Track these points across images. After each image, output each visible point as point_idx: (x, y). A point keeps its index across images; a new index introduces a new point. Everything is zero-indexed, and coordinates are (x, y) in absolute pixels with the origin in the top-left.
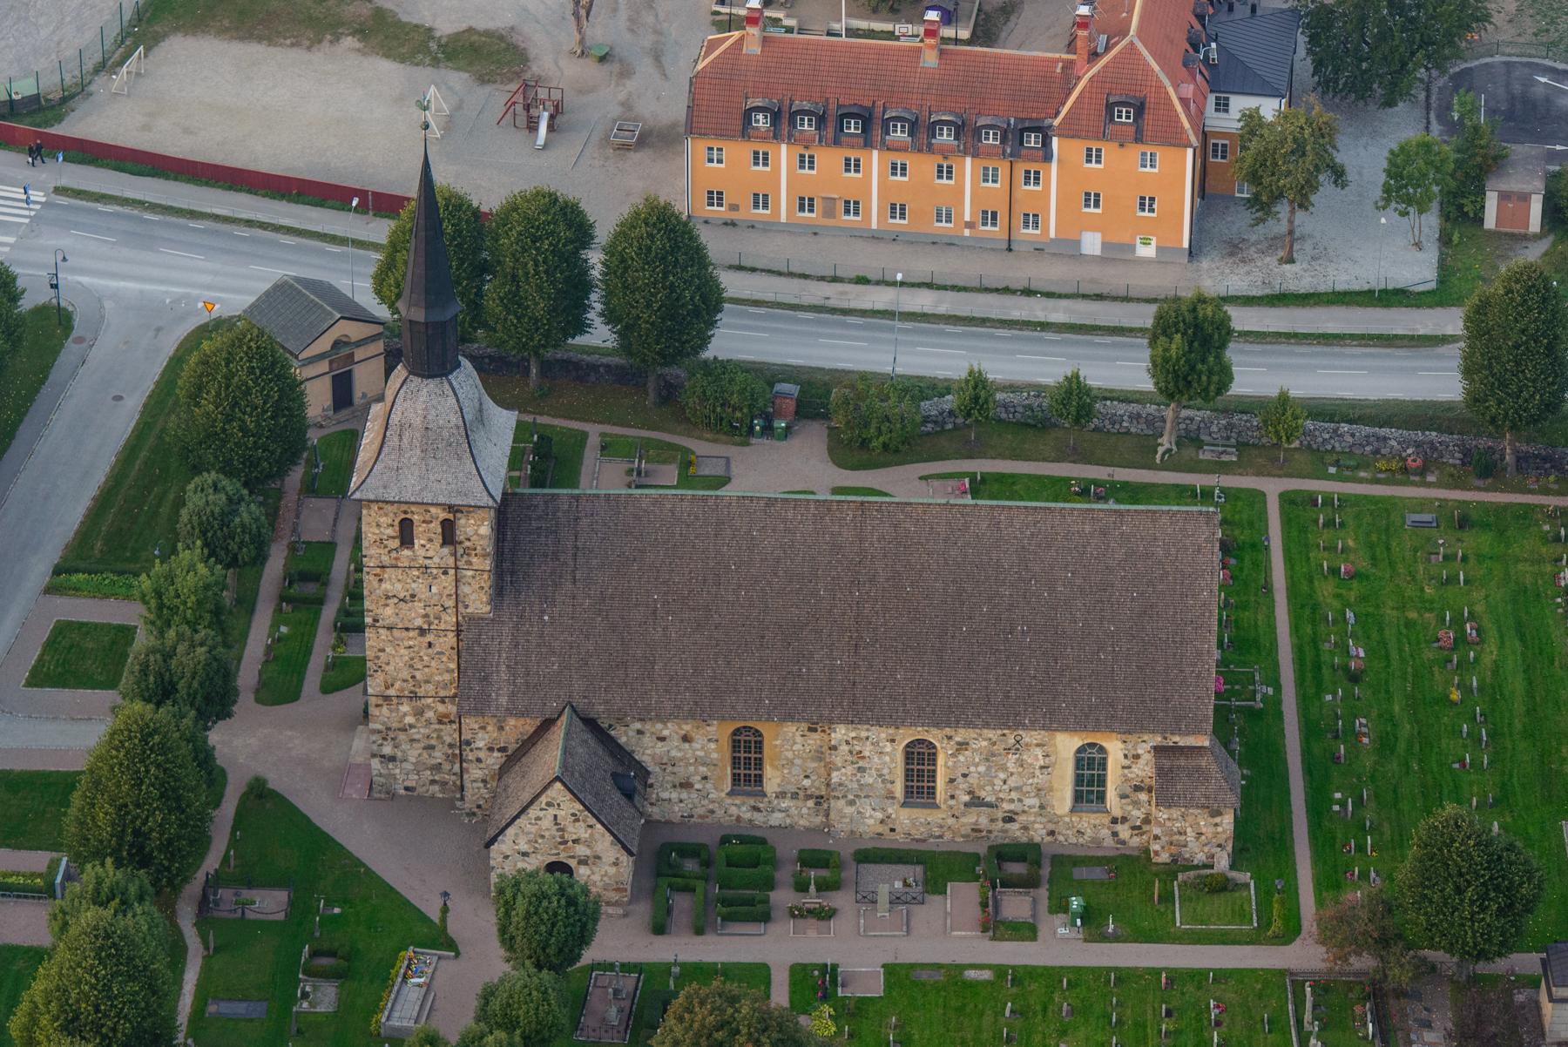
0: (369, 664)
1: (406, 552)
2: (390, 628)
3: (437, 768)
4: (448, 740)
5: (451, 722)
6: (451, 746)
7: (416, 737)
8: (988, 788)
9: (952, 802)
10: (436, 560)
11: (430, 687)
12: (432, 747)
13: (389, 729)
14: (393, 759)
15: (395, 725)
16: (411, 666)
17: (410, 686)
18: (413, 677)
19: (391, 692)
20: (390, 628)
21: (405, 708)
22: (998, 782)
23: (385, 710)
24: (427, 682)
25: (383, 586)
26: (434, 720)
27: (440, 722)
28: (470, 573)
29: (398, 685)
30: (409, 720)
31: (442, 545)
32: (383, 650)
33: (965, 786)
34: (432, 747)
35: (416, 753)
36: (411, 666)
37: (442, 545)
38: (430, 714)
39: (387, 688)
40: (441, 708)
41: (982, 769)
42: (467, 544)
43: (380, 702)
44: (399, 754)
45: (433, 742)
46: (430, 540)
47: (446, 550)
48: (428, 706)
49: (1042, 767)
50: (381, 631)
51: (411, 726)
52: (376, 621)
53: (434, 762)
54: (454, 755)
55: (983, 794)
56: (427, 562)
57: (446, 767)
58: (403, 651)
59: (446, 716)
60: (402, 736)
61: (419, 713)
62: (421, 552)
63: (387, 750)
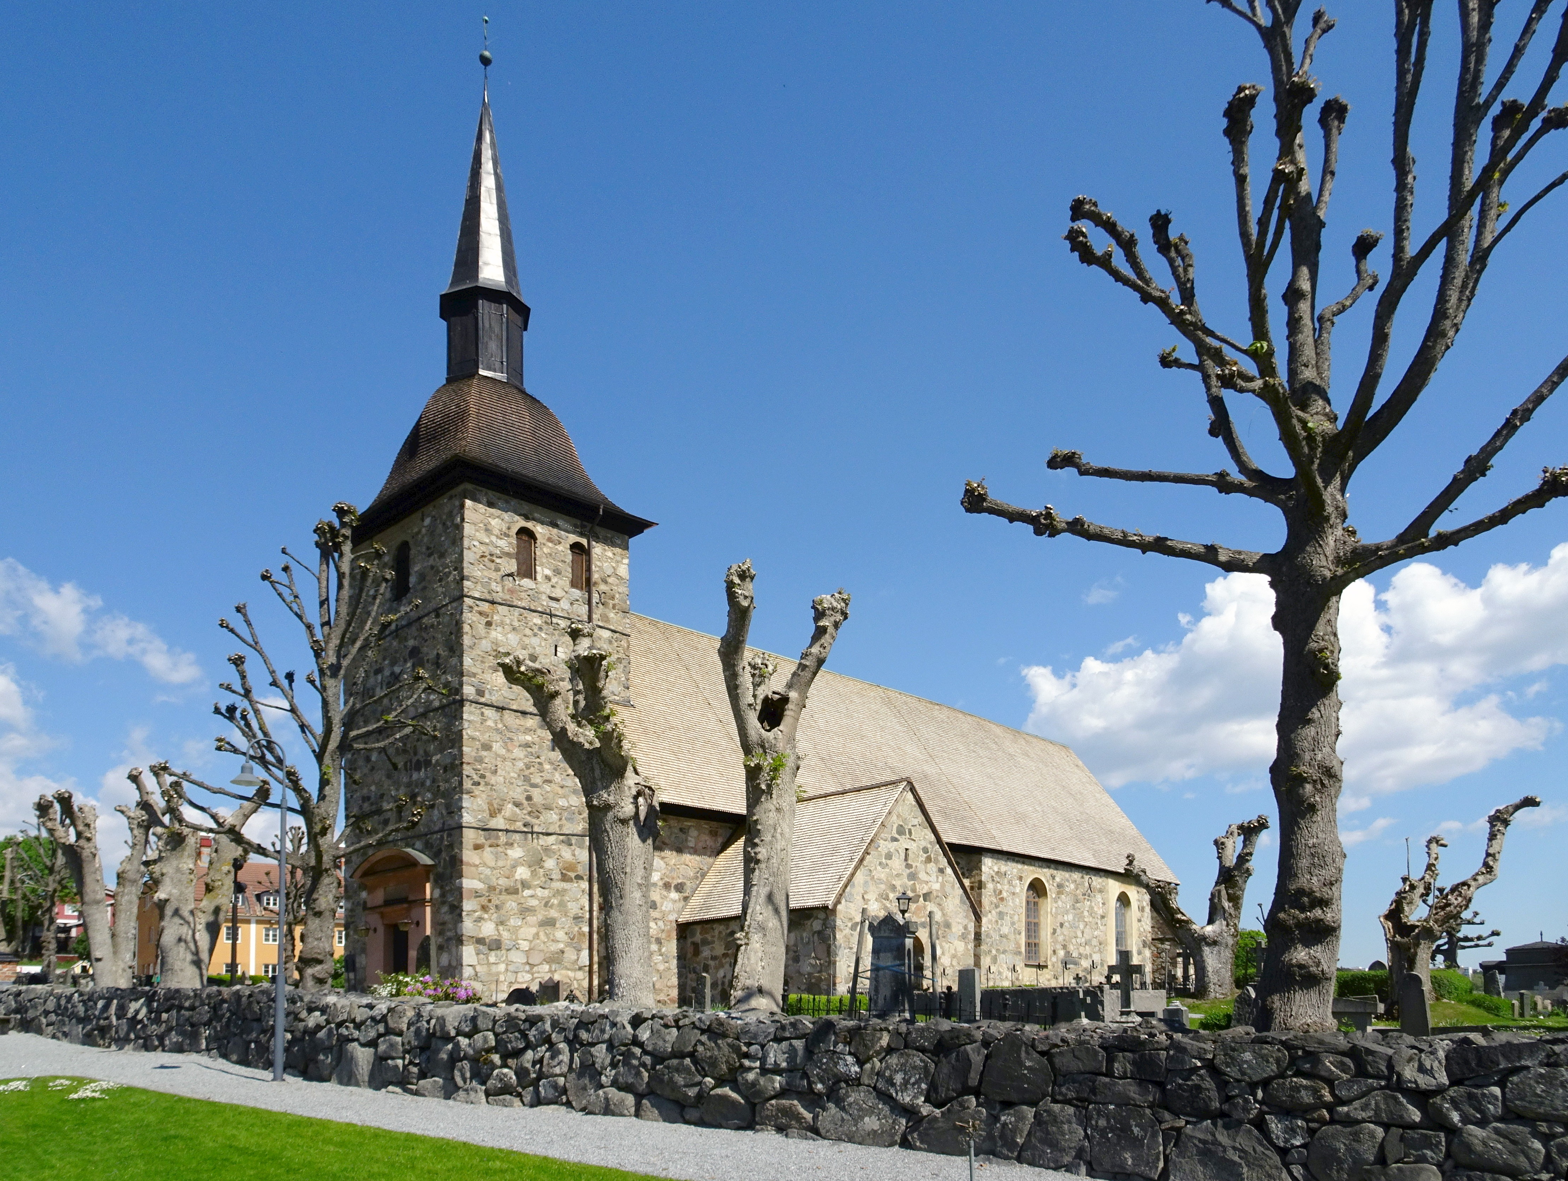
0: (467, 770)
1: (526, 582)
2: (501, 709)
3: (556, 958)
4: (573, 908)
5: (579, 877)
6: (577, 918)
7: (534, 902)
8: (1074, 941)
9: (1054, 959)
10: (564, 604)
11: (553, 816)
12: (550, 923)
13: (492, 889)
14: (496, 945)
15: (503, 882)
16: (527, 779)
17: (522, 814)
18: (529, 798)
19: (498, 822)
20: (501, 709)
21: (516, 853)
22: (1079, 934)
23: (488, 852)
24: (548, 808)
25: (493, 634)
26: (556, 875)
27: (565, 878)
28: (606, 634)
29: (509, 808)
30: (523, 873)
31: (573, 584)
32: (487, 747)
33: (1061, 938)
34: (550, 923)
35: (528, 932)
36: (527, 779)
37: (573, 584)
38: (550, 863)
39: (493, 814)
40: (566, 854)
41: (1070, 917)
42: (603, 587)
43: (481, 840)
44: (505, 935)
45: (553, 913)
46: (557, 572)
47: (577, 593)
48: (547, 850)
49: (1103, 917)
50: (489, 712)
51: (525, 885)
52: (480, 693)
53: (555, 947)
54: (582, 934)
55: (1071, 948)
56: (553, 604)
57: (570, 955)
58: (518, 753)
59: (571, 867)
60: (511, 904)
61: (536, 863)
62: (545, 588)
63: (488, 929)
